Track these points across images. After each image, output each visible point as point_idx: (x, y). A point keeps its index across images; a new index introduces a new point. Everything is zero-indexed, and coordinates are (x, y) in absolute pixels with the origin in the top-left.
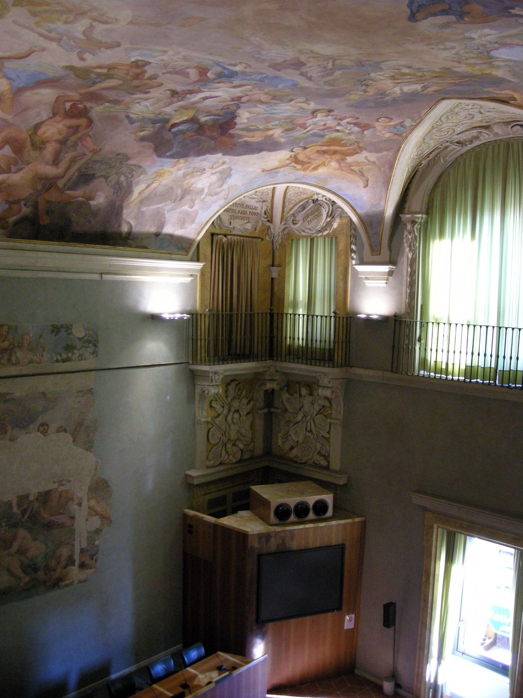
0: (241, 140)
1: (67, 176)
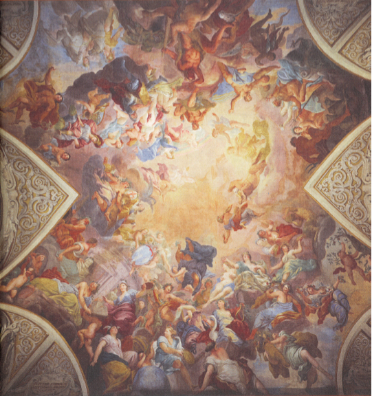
1: (168, 27)
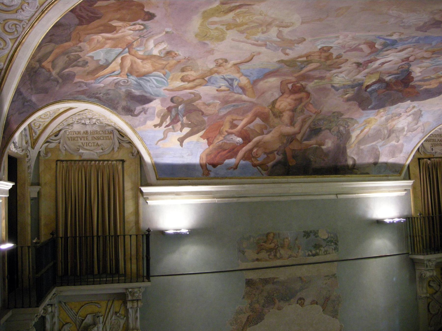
0: (422, 89)
1: (302, 132)
